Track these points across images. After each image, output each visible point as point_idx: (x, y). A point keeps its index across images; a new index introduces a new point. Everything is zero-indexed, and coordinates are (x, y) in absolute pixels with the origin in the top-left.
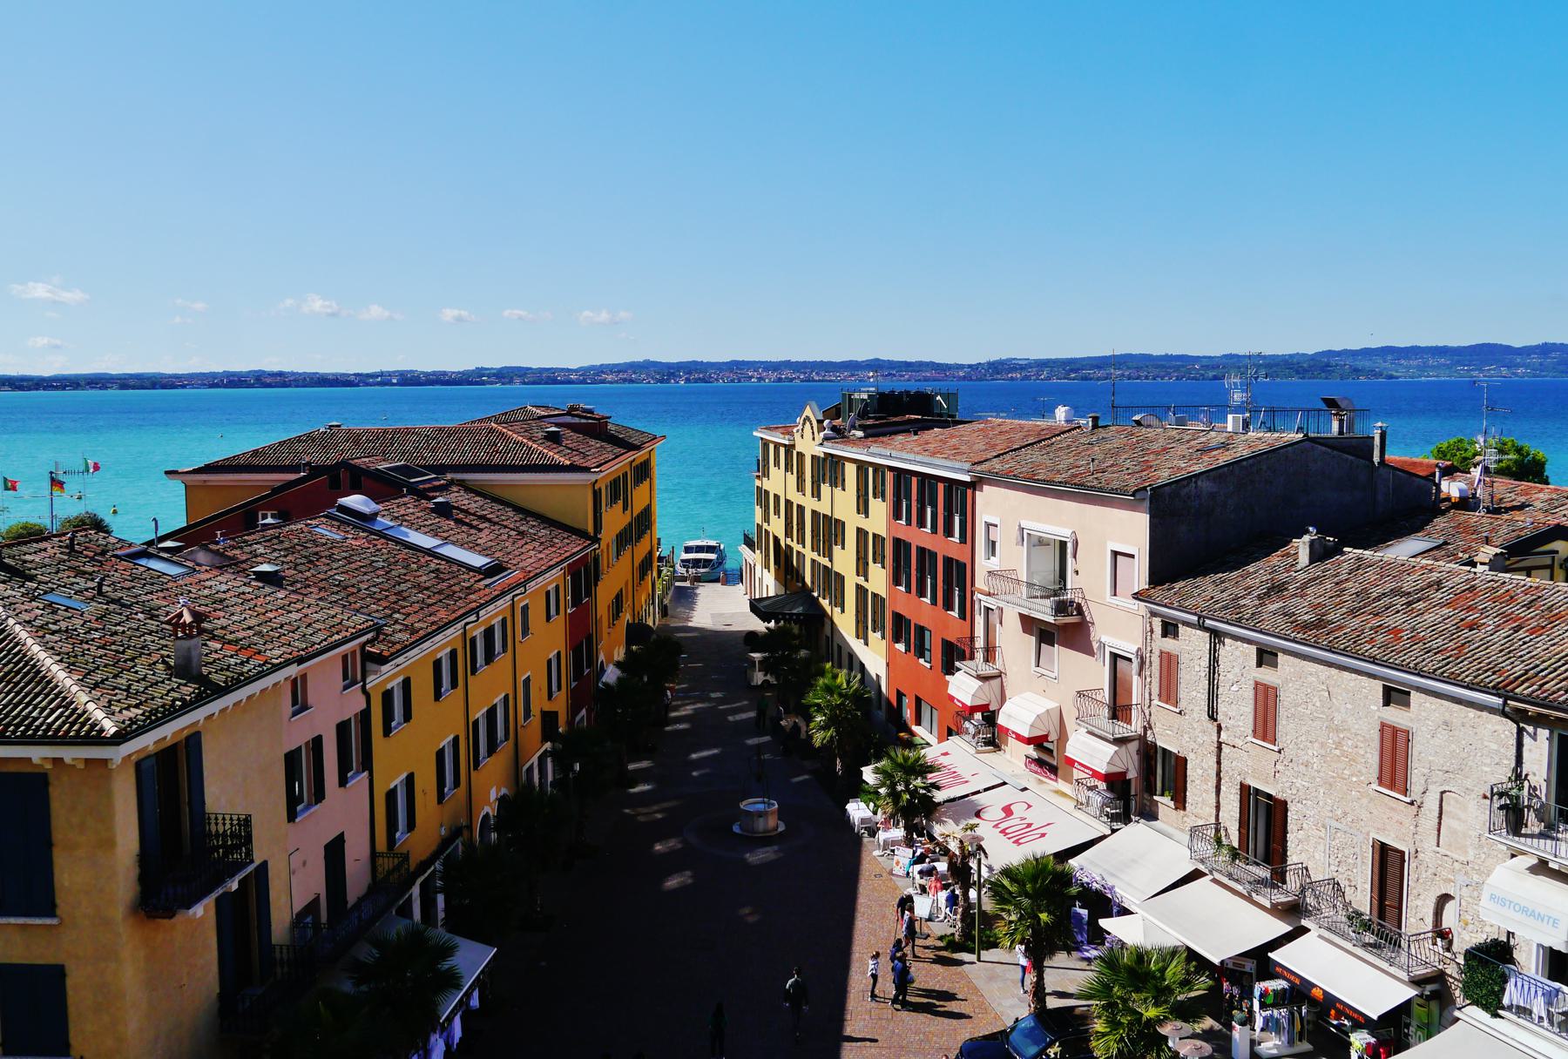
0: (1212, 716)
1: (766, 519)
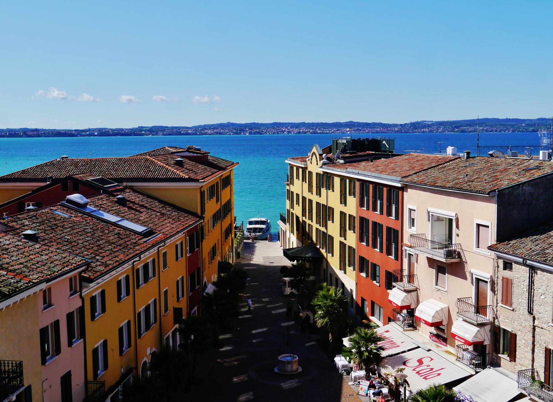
0: (530, 312)
1: (292, 206)
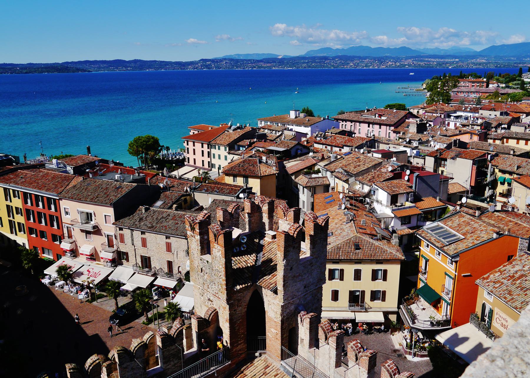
0: (133, 245)
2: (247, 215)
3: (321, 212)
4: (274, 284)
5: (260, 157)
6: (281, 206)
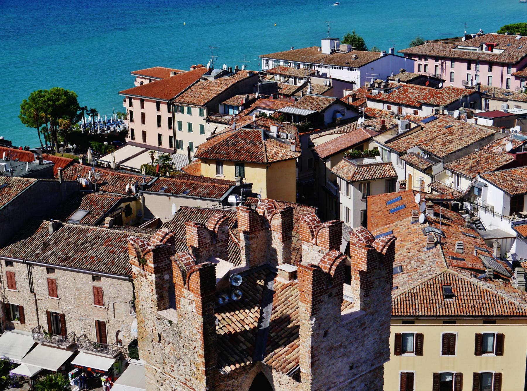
0: (32, 291)
2: (242, 236)
3: (381, 228)
4: (294, 363)
5: (265, 127)
6: (306, 218)
